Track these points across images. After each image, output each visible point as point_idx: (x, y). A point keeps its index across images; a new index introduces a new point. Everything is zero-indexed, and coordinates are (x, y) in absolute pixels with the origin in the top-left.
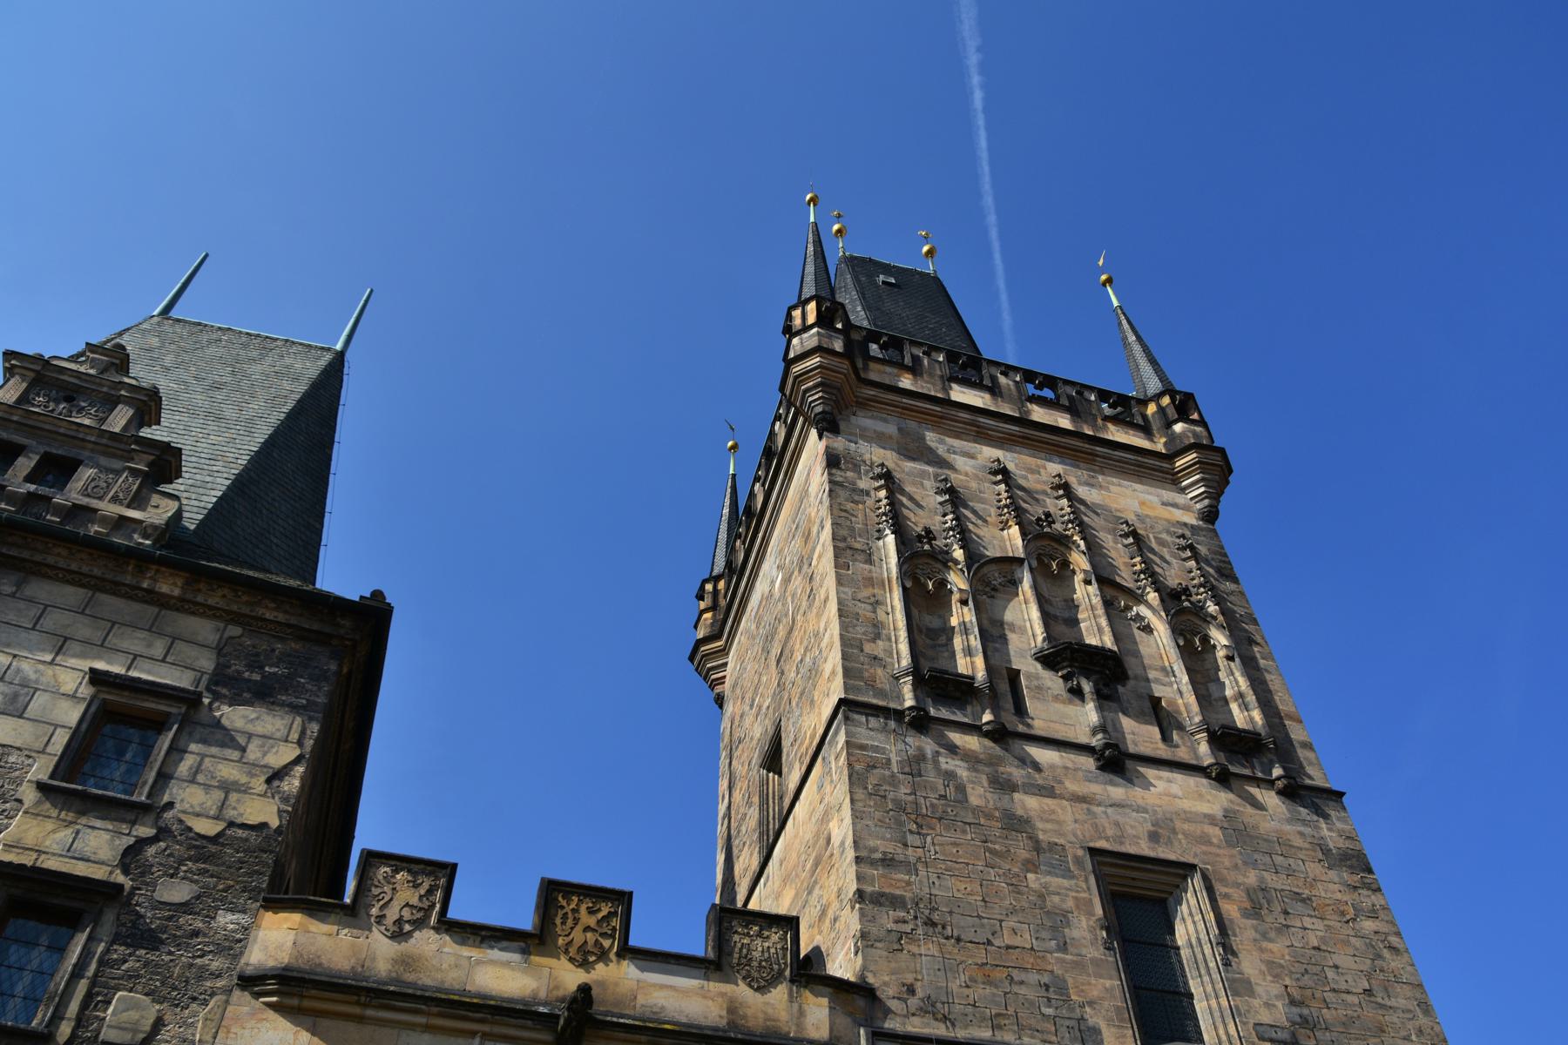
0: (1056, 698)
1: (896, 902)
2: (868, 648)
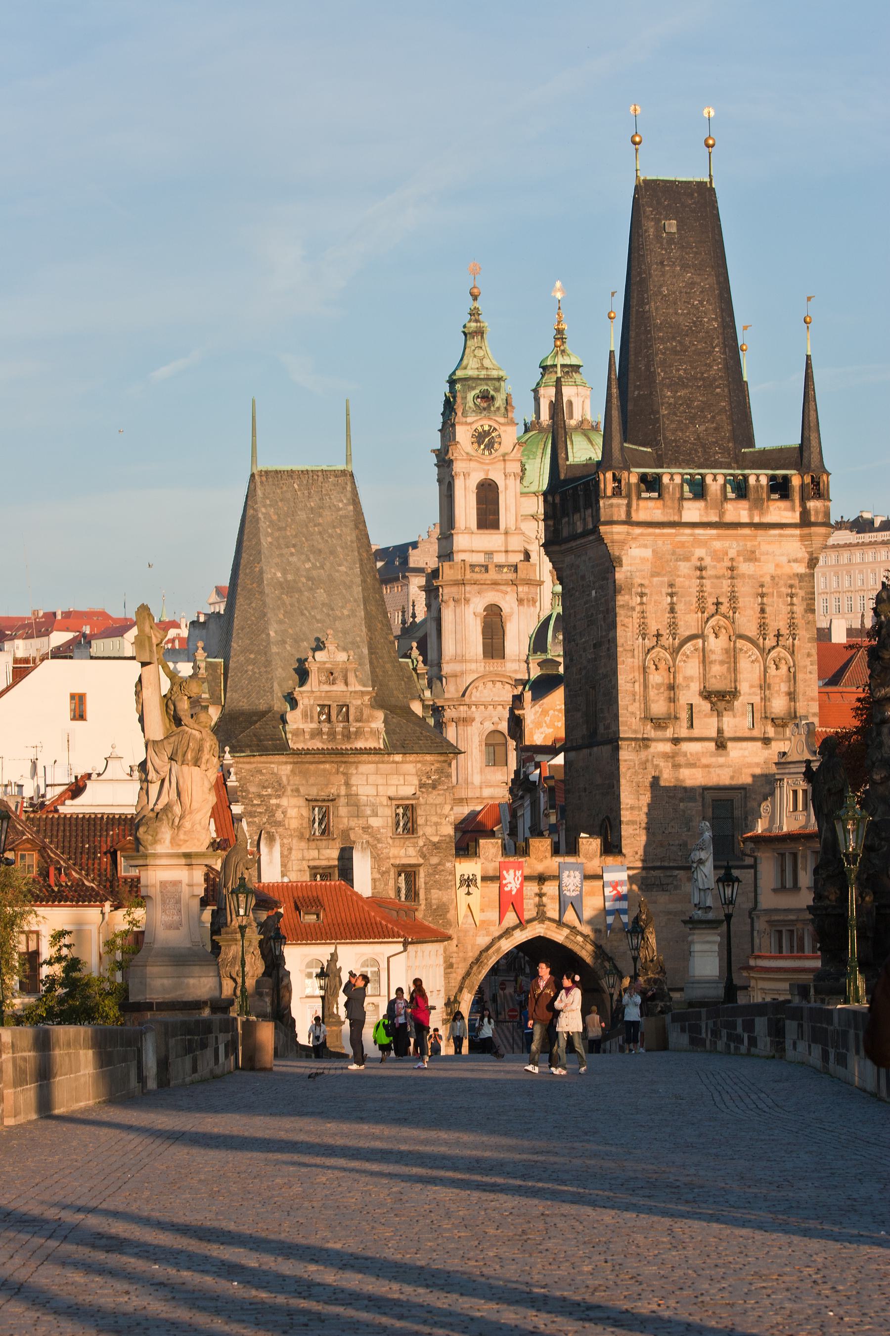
0: (705, 716)
1: (633, 822)
2: (630, 710)
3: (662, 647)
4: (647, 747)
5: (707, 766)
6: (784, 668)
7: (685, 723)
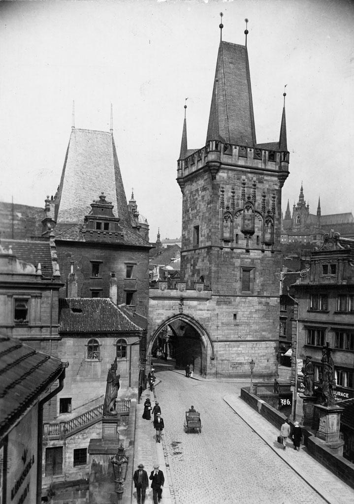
3: (229, 212)
4: (222, 249)
5: (243, 258)
6: (270, 224)
7: (235, 242)
